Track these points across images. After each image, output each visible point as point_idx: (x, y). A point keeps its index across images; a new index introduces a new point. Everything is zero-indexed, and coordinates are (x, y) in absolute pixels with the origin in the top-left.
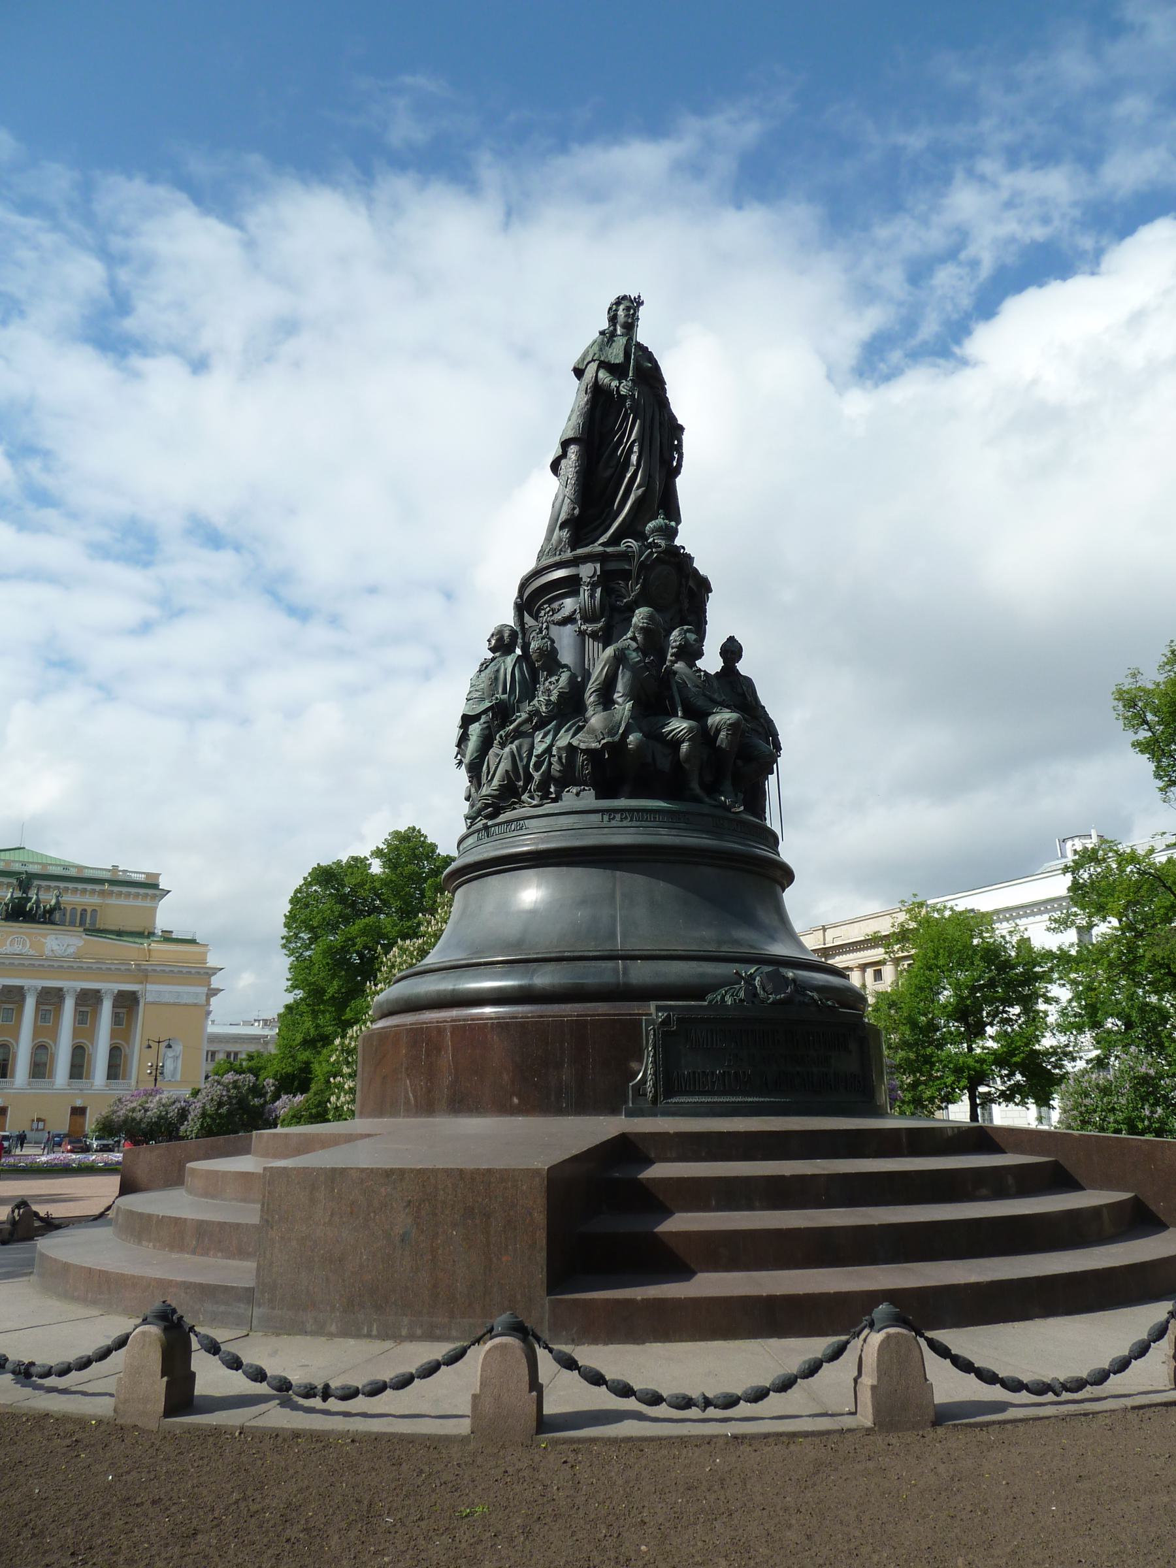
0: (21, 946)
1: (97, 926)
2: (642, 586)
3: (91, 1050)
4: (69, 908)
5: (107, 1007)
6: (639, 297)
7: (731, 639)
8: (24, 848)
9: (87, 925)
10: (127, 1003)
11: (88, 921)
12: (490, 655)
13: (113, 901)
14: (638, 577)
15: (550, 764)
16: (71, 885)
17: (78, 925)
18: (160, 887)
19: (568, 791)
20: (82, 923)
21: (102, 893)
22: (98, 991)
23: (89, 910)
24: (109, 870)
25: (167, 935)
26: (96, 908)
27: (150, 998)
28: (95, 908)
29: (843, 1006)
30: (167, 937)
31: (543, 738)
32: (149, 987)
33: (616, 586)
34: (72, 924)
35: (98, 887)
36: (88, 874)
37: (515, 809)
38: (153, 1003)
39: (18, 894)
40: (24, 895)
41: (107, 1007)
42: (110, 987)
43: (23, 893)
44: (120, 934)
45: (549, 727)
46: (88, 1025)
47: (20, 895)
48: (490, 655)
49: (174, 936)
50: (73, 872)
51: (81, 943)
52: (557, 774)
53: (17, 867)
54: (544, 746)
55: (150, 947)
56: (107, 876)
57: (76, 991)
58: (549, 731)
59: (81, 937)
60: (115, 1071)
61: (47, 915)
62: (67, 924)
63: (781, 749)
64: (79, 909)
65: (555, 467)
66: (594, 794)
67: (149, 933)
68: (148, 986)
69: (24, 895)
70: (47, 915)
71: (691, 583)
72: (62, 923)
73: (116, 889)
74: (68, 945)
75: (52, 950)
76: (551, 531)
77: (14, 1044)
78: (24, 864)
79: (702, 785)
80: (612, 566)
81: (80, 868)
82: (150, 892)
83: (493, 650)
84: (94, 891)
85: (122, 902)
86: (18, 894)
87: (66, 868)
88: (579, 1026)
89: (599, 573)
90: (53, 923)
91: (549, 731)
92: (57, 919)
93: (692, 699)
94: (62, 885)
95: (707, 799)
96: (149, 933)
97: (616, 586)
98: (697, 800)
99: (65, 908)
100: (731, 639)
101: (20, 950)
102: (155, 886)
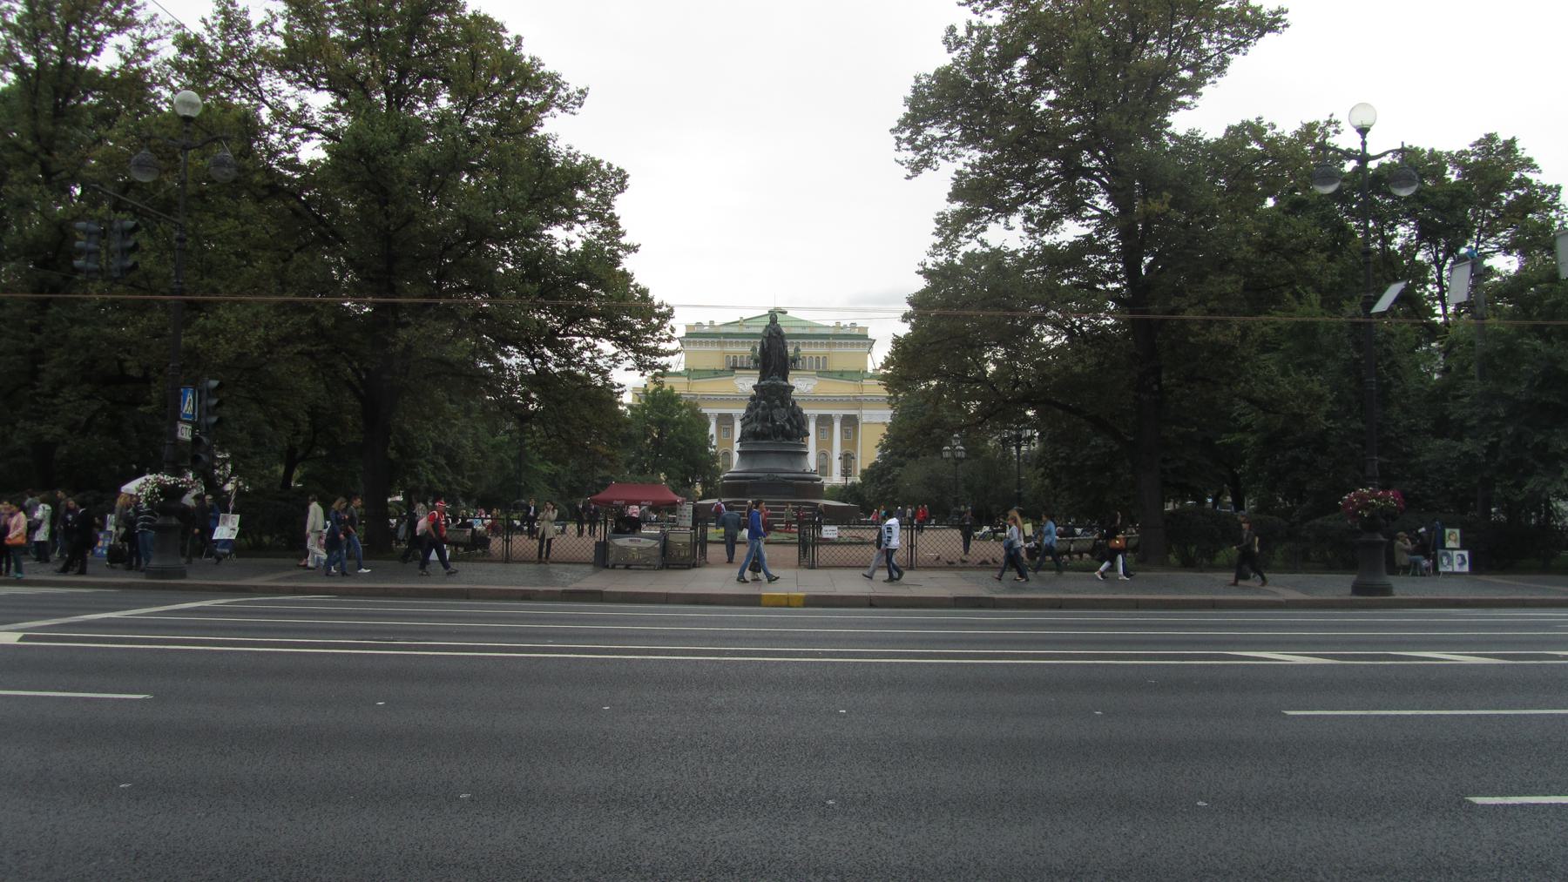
5: (837, 426)
10: (850, 423)
13: (836, 350)
20: (818, 366)
21: (828, 344)
23: (821, 357)
35: (825, 341)
36: (818, 331)
41: (837, 426)
42: (837, 412)
44: (842, 375)
51: (816, 383)
56: (831, 332)
60: (846, 472)
73: (837, 341)
82: (861, 342)
84: (822, 344)
85: (844, 350)
87: (804, 327)
88: (740, 484)
94: (801, 341)
102: (865, 337)
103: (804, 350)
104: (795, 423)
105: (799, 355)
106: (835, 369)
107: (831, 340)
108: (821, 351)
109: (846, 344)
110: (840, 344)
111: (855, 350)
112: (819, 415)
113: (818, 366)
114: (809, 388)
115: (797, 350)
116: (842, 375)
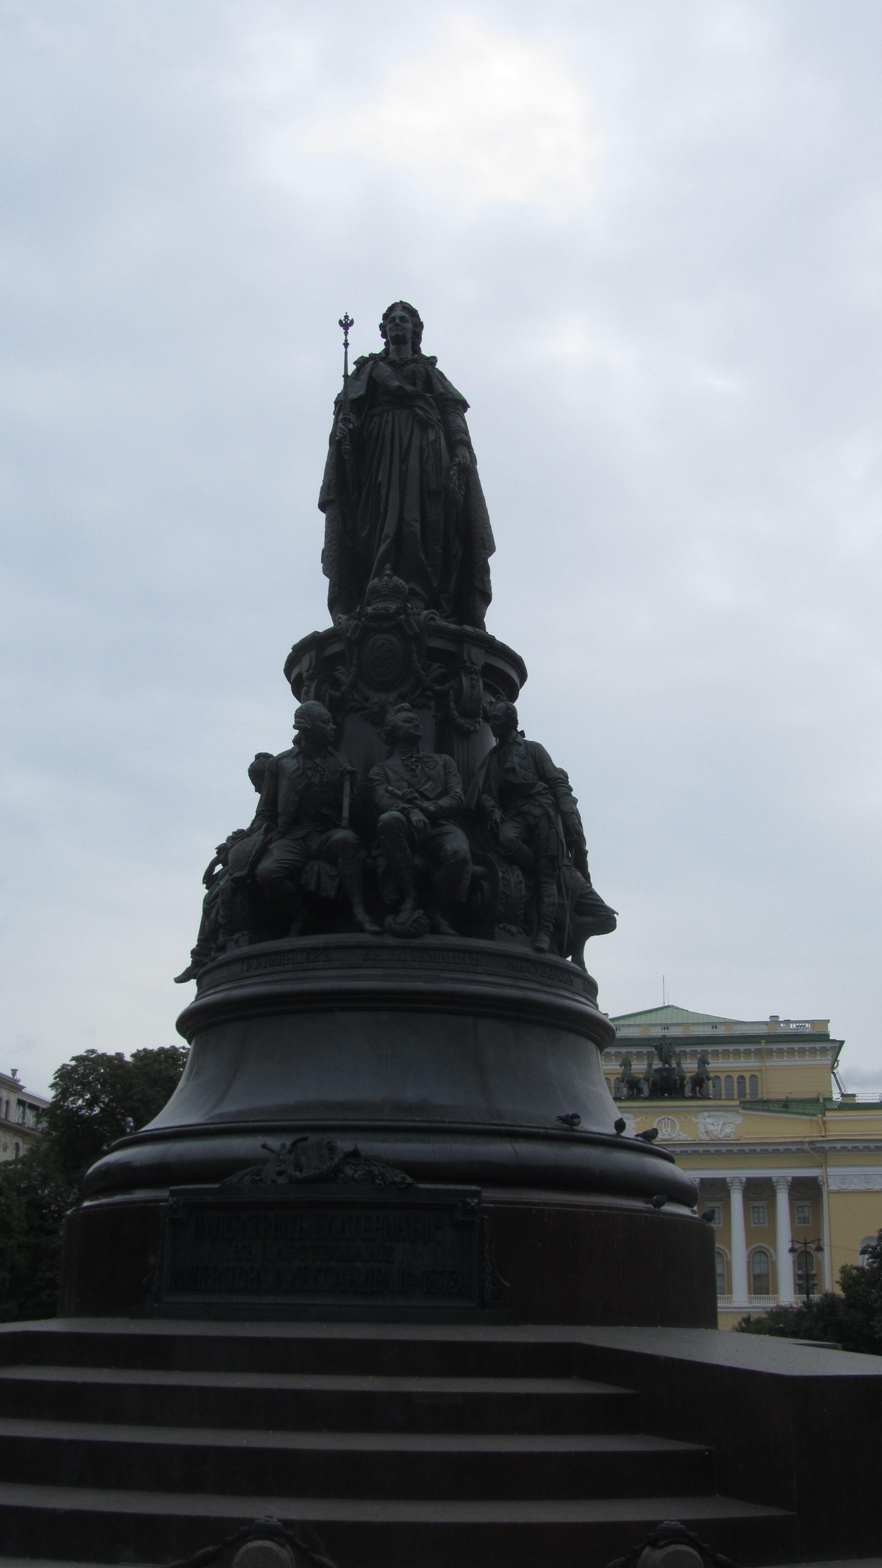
0: (669, 1130)
1: (760, 1097)
3: (774, 1257)
4: (723, 1076)
5: (782, 1199)
6: (346, 317)
8: (668, 1007)
9: (748, 1097)
11: (748, 1091)
13: (774, 1062)
15: (218, 912)
16: (720, 1048)
17: (736, 1097)
18: (831, 1038)
21: (759, 1052)
22: (723, 1180)
23: (747, 1076)
24: (766, 1023)
25: (849, 1101)
26: (757, 1074)
27: (833, 1187)
28: (754, 1073)
29: (420, 1178)
30: (849, 1104)
32: (831, 1171)
33: (337, 673)
34: (730, 1097)
35: (753, 1047)
36: (738, 1031)
38: (838, 1192)
39: (657, 1064)
40: (667, 1066)
41: (782, 1199)
43: (666, 1062)
44: (786, 1105)
46: (766, 1225)
47: (661, 1066)
49: (860, 1099)
50: (721, 1031)
51: (739, 1120)
52: (221, 920)
53: (657, 1032)
55: (825, 1119)
57: (741, 1181)
59: (737, 1112)
61: (698, 1089)
62: (723, 1097)
64: (735, 1076)
67: (825, 1099)
68: (829, 1170)
69: (667, 1066)
70: (698, 1089)
72: (718, 1097)
73: (775, 1047)
74: (724, 1124)
75: (707, 1132)
77: (727, 1251)
78: (666, 1027)
81: (715, 1023)
82: (818, 1045)
84: (748, 1053)
85: (786, 1061)
86: (657, 1064)
87: (714, 1025)
89: (313, 664)
90: (707, 1098)
92: (711, 1092)
94: (710, 1049)
96: (825, 1099)
98: (362, 930)
99: (717, 1077)
101: (669, 1135)
102: (825, 1037)
103: (715, 1065)
104: (510, 831)
105: (706, 1072)
106: (773, 1096)
107: (763, 1045)
108: (747, 1064)
109: (791, 1052)
110: (781, 1052)
111: (807, 1061)
112: (749, 1180)
113: (742, 1094)
114: (728, 1130)
115: (703, 1062)
116: (786, 1105)
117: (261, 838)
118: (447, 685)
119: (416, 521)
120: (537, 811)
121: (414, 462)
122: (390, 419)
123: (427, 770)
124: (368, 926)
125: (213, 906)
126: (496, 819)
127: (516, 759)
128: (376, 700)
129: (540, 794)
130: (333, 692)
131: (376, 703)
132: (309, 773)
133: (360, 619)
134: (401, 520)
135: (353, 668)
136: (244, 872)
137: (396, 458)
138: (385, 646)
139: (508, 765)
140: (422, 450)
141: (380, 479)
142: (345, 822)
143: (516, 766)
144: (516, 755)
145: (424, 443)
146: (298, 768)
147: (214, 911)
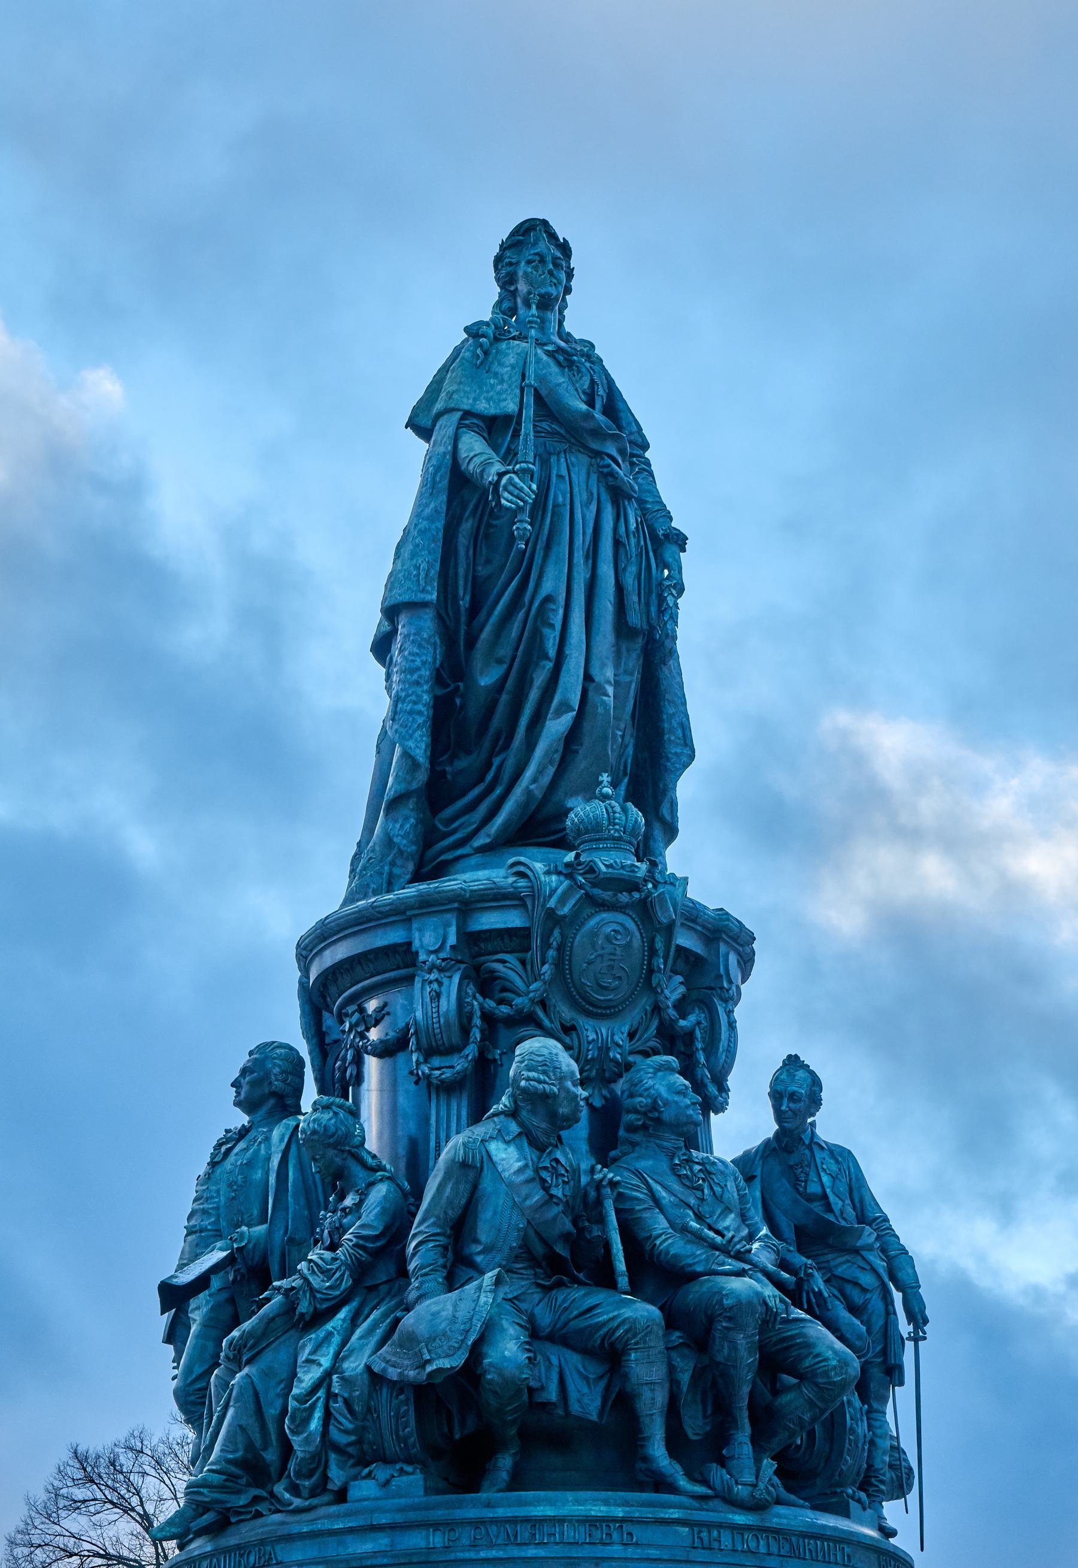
2: (559, 964)
7: (793, 1062)
12: (242, 1119)
14: (546, 945)
15: (328, 1415)
19: (369, 1476)
31: (314, 1352)
33: (499, 966)
37: (259, 1515)
45: (329, 1326)
48: (242, 1119)
52: (342, 1439)
54: (315, 1373)
58: (330, 1334)
63: (926, 1321)
65: (381, 648)
66: (421, 1483)
71: (685, 940)
76: (369, 828)
79: (676, 1443)
80: (490, 920)
83: (247, 1104)
89: (452, 940)
91: (330, 1334)
93: (658, 1242)
95: (683, 1483)
97: (499, 966)
100: (793, 1062)
117: (486, 1299)
118: (692, 1018)
119: (609, 682)
120: (867, 1279)
121: (606, 570)
122: (564, 472)
123: (717, 1189)
124: (683, 1483)
125: (313, 1407)
126: (820, 1290)
127: (825, 1179)
128: (592, 1036)
129: (869, 1248)
130: (490, 1003)
131: (593, 1040)
132: (545, 1174)
133: (570, 876)
134: (588, 677)
135: (546, 966)
136: (457, 1361)
137: (579, 557)
138: (619, 937)
139: (814, 1188)
140: (617, 543)
141: (547, 588)
142: (623, 1281)
143: (828, 1191)
144: (824, 1170)
145: (622, 530)
146: (526, 1166)
147: (318, 1414)
